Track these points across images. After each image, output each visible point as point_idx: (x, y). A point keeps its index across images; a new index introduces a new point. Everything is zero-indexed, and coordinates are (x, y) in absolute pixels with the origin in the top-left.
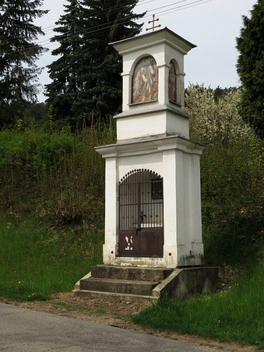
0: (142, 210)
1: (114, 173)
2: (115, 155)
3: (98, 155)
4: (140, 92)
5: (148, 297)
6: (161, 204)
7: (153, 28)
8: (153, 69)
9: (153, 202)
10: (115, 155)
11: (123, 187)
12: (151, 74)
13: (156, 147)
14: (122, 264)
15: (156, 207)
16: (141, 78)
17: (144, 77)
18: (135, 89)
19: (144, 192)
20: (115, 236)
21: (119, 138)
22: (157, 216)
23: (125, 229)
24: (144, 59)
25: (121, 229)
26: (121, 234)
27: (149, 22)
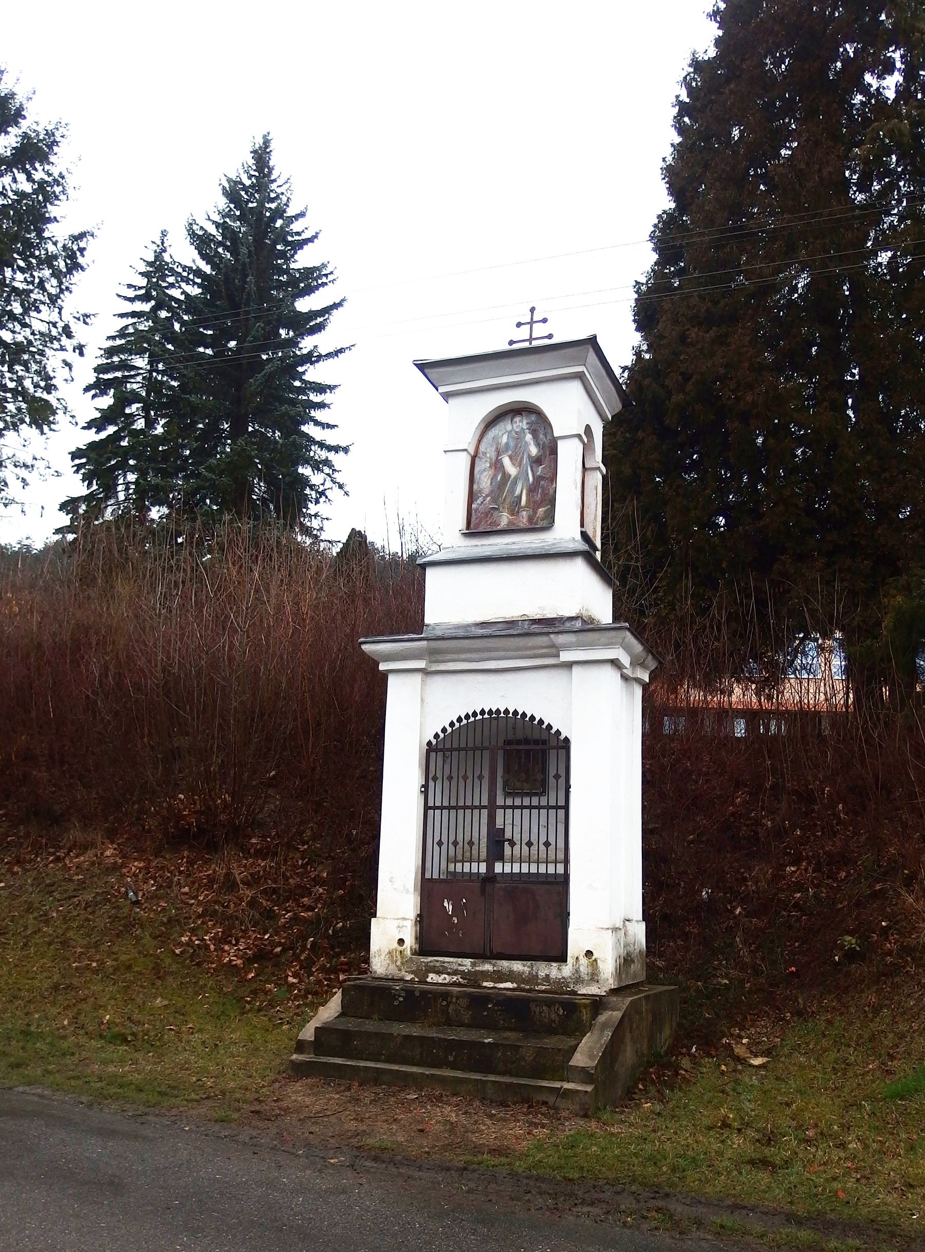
0: (499, 824)
1: (416, 711)
2: (421, 664)
3: (372, 663)
4: (494, 500)
5: (557, 1085)
6: (561, 813)
7: (531, 339)
8: (537, 444)
9: (509, 802)
10: (421, 664)
11: (447, 753)
12: (529, 456)
13: (555, 651)
14: (432, 978)
15: (476, 818)
16: (497, 465)
17: (506, 461)
18: (480, 492)
19: (470, 774)
20: (412, 896)
21: (430, 617)
22: (440, 843)
23: (435, 876)
24: (509, 417)
25: (428, 876)
26: (429, 890)
27: (519, 325)
